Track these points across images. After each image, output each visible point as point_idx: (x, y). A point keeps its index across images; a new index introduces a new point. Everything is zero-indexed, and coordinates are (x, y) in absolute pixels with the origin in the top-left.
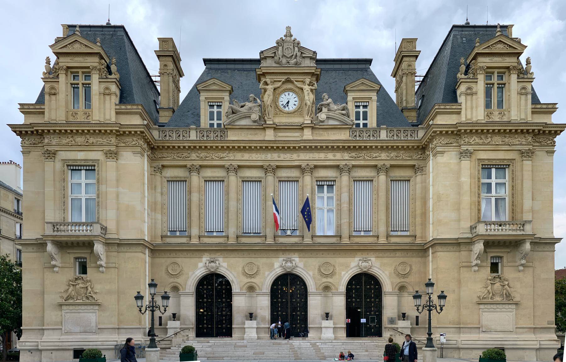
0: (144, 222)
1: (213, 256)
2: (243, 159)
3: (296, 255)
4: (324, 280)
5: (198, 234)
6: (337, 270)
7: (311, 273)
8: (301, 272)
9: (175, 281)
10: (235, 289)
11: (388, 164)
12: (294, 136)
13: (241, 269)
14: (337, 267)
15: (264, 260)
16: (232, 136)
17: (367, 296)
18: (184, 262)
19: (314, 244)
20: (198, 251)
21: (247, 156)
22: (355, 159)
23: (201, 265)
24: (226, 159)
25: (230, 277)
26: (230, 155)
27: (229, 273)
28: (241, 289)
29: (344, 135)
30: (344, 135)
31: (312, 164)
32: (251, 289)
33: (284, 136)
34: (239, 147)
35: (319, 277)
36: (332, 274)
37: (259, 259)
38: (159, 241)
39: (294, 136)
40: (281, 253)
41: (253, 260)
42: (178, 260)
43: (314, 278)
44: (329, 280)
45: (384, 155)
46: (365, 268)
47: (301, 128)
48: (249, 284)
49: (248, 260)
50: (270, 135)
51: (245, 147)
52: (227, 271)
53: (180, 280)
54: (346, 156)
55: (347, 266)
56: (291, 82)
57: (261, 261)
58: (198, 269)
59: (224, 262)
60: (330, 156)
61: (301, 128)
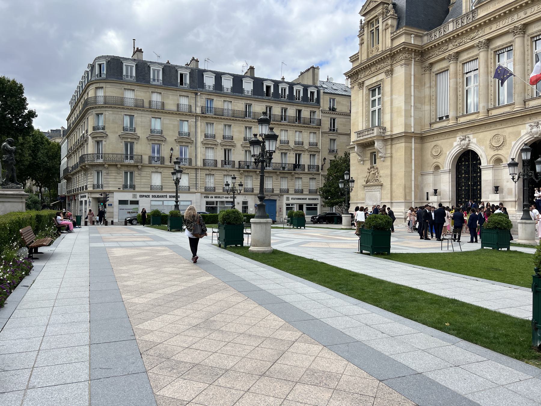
0: (411, 116)
1: (465, 134)
2: (492, 30)
5: (455, 115)
9: (437, 161)
13: (488, 142)
15: (510, 130)
18: (442, 143)
21: (494, 27)
23: (455, 144)
24: (477, 37)
25: (480, 151)
26: (479, 33)
27: (478, 148)
28: (489, 162)
32: (498, 161)
34: (485, 22)
37: (505, 129)
38: (427, 128)
40: (528, 119)
41: (500, 131)
42: (439, 143)
48: (495, 157)
49: (495, 132)
51: (490, 20)
52: (476, 147)
53: (440, 160)
57: (507, 131)
58: (452, 148)
59: (474, 138)
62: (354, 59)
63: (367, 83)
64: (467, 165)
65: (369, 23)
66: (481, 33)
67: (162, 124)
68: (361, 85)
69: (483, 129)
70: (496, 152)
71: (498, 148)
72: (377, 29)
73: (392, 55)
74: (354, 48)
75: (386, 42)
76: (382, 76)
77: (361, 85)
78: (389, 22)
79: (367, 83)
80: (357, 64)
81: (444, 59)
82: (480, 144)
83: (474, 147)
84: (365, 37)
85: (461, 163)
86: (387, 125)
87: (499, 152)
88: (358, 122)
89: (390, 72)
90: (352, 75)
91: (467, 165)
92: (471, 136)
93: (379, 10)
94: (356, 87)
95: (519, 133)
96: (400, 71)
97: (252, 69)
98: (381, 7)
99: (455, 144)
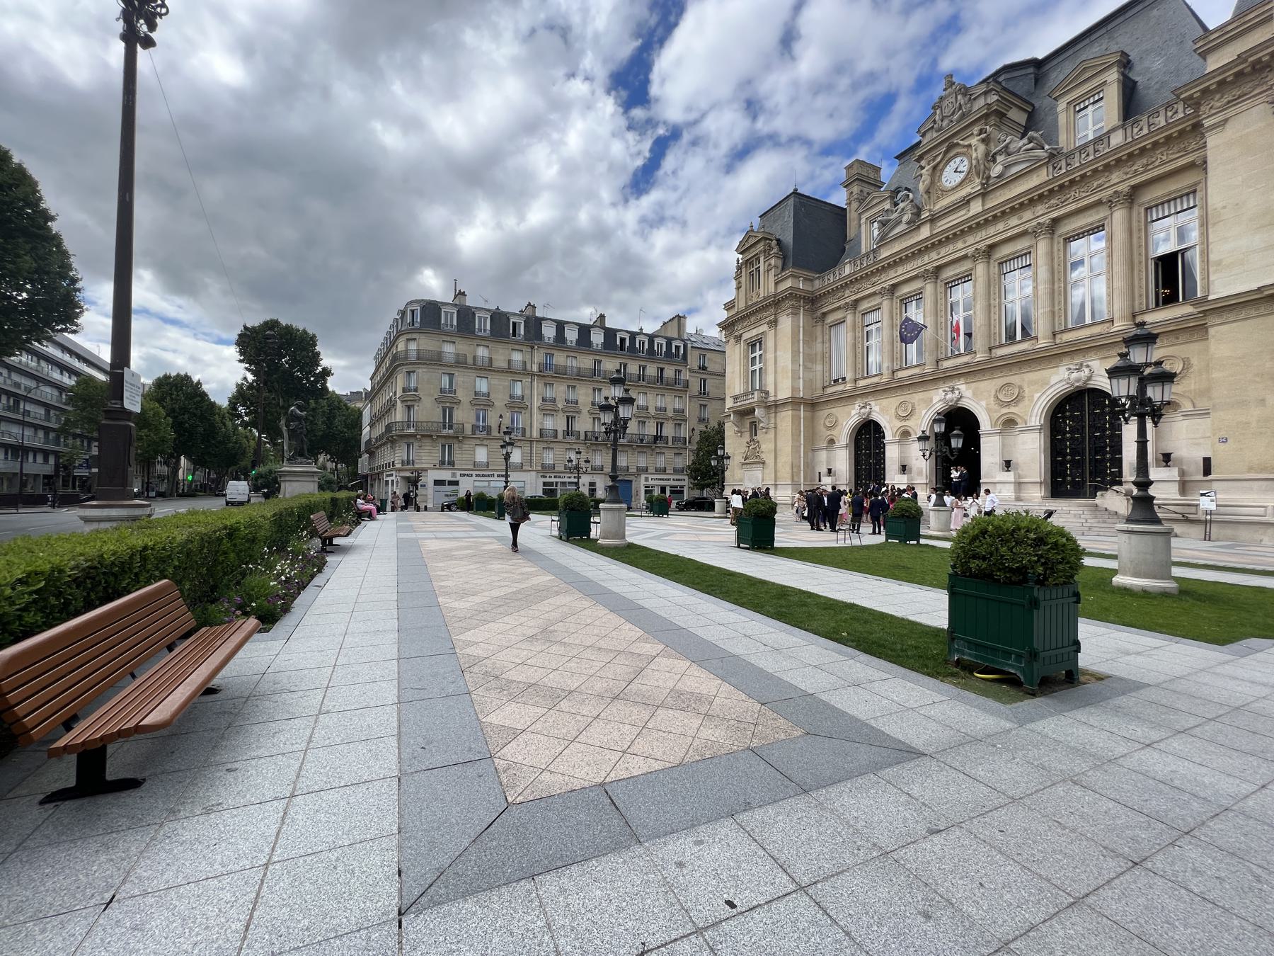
3: (962, 381)
4: (1005, 411)
6: (1027, 393)
7: (984, 403)
8: (967, 403)
10: (888, 436)
11: (1124, 188)
12: (961, 216)
14: (1027, 390)
16: (885, 253)
17: (1094, 427)
19: (992, 360)
20: (848, 398)
21: (900, 270)
22: (1057, 207)
23: (853, 412)
28: (894, 436)
29: (1041, 177)
30: (1041, 177)
31: (982, 246)
32: (906, 434)
33: (943, 225)
35: (996, 407)
36: (1017, 400)
38: (819, 393)
39: (961, 216)
41: (907, 398)
42: (833, 411)
43: (988, 410)
44: (1013, 409)
45: (1115, 177)
46: (1078, 380)
47: (966, 202)
49: (902, 399)
50: (925, 232)
53: (835, 432)
54: (1040, 209)
55: (1045, 382)
56: (958, 144)
57: (916, 397)
58: (849, 417)
60: (1014, 221)
61: (966, 202)
62: (729, 306)
63: (745, 336)
64: (868, 439)
65: (748, 263)
66: (884, 277)
67: (489, 385)
68: (738, 338)
69: (979, 377)
70: (1005, 411)
71: (905, 418)
72: (758, 270)
73: (776, 303)
74: (730, 293)
75: (768, 286)
76: (764, 328)
77: (738, 338)
78: (773, 262)
79: (745, 336)
80: (733, 312)
81: (839, 308)
82: (884, 413)
83: (876, 417)
84: (743, 279)
85: (1064, 413)
86: (771, 389)
87: (907, 423)
88: (735, 383)
89: (774, 323)
90: (727, 326)
91: (868, 439)
92: (873, 403)
93: (760, 247)
94: (732, 341)
95: (931, 400)
96: (786, 322)
97: (602, 317)
98: (762, 244)
99: (853, 412)
